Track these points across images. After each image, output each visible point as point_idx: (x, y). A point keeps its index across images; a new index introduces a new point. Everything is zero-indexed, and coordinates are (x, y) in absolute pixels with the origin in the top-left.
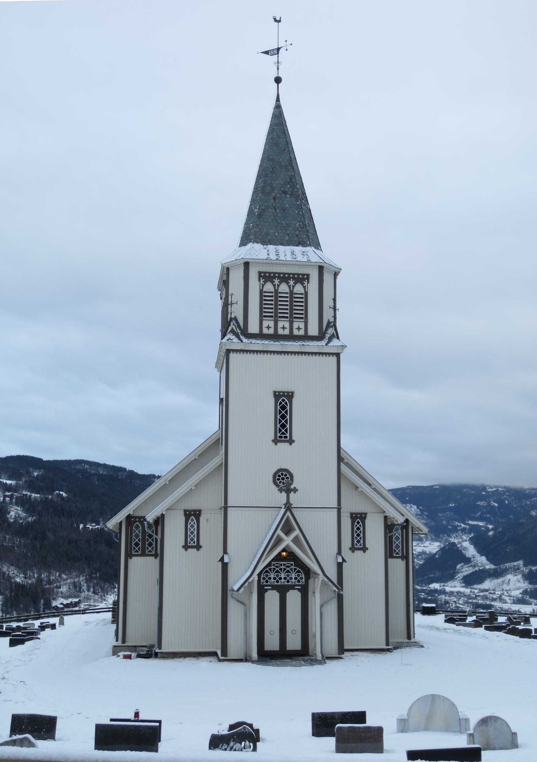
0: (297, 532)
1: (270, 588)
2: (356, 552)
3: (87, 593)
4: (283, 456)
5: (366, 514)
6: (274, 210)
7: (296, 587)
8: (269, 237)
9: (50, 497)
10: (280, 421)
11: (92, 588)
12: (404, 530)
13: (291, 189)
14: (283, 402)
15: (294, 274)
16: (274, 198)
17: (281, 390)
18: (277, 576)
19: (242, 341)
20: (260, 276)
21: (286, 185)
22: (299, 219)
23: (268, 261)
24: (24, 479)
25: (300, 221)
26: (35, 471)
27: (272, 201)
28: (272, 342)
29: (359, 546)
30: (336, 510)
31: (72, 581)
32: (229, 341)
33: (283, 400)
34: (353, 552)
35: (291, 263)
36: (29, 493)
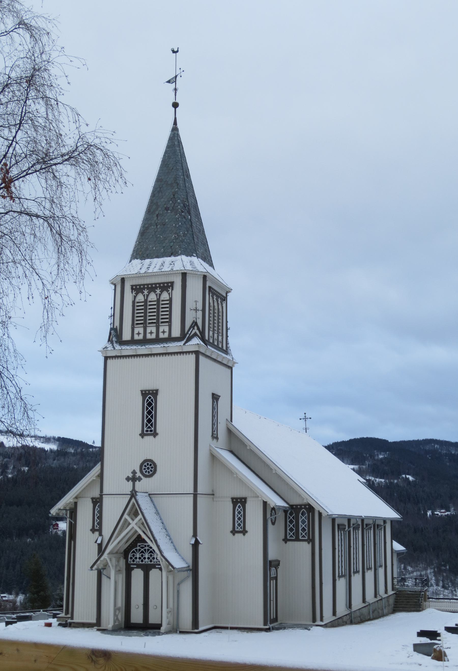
0: (140, 516)
1: (135, 566)
2: (236, 535)
3: (435, 587)
4: (149, 448)
5: (245, 499)
6: (156, 226)
7: (157, 566)
8: (148, 252)
9: (396, 481)
10: (152, 417)
11: (441, 582)
12: (311, 514)
13: (172, 205)
14: (150, 398)
15: (159, 284)
16: (157, 216)
17: (150, 389)
18: (142, 556)
19: (114, 349)
20: (132, 289)
21: (169, 201)
22: (175, 231)
23: (137, 275)
24: (367, 463)
25: (175, 233)
26: (381, 454)
27: (155, 218)
28: (139, 347)
29: (239, 529)
30: (192, 495)
31: (419, 573)
32: (105, 349)
33: (150, 398)
34: (234, 535)
35: (157, 274)
36: (373, 479)
